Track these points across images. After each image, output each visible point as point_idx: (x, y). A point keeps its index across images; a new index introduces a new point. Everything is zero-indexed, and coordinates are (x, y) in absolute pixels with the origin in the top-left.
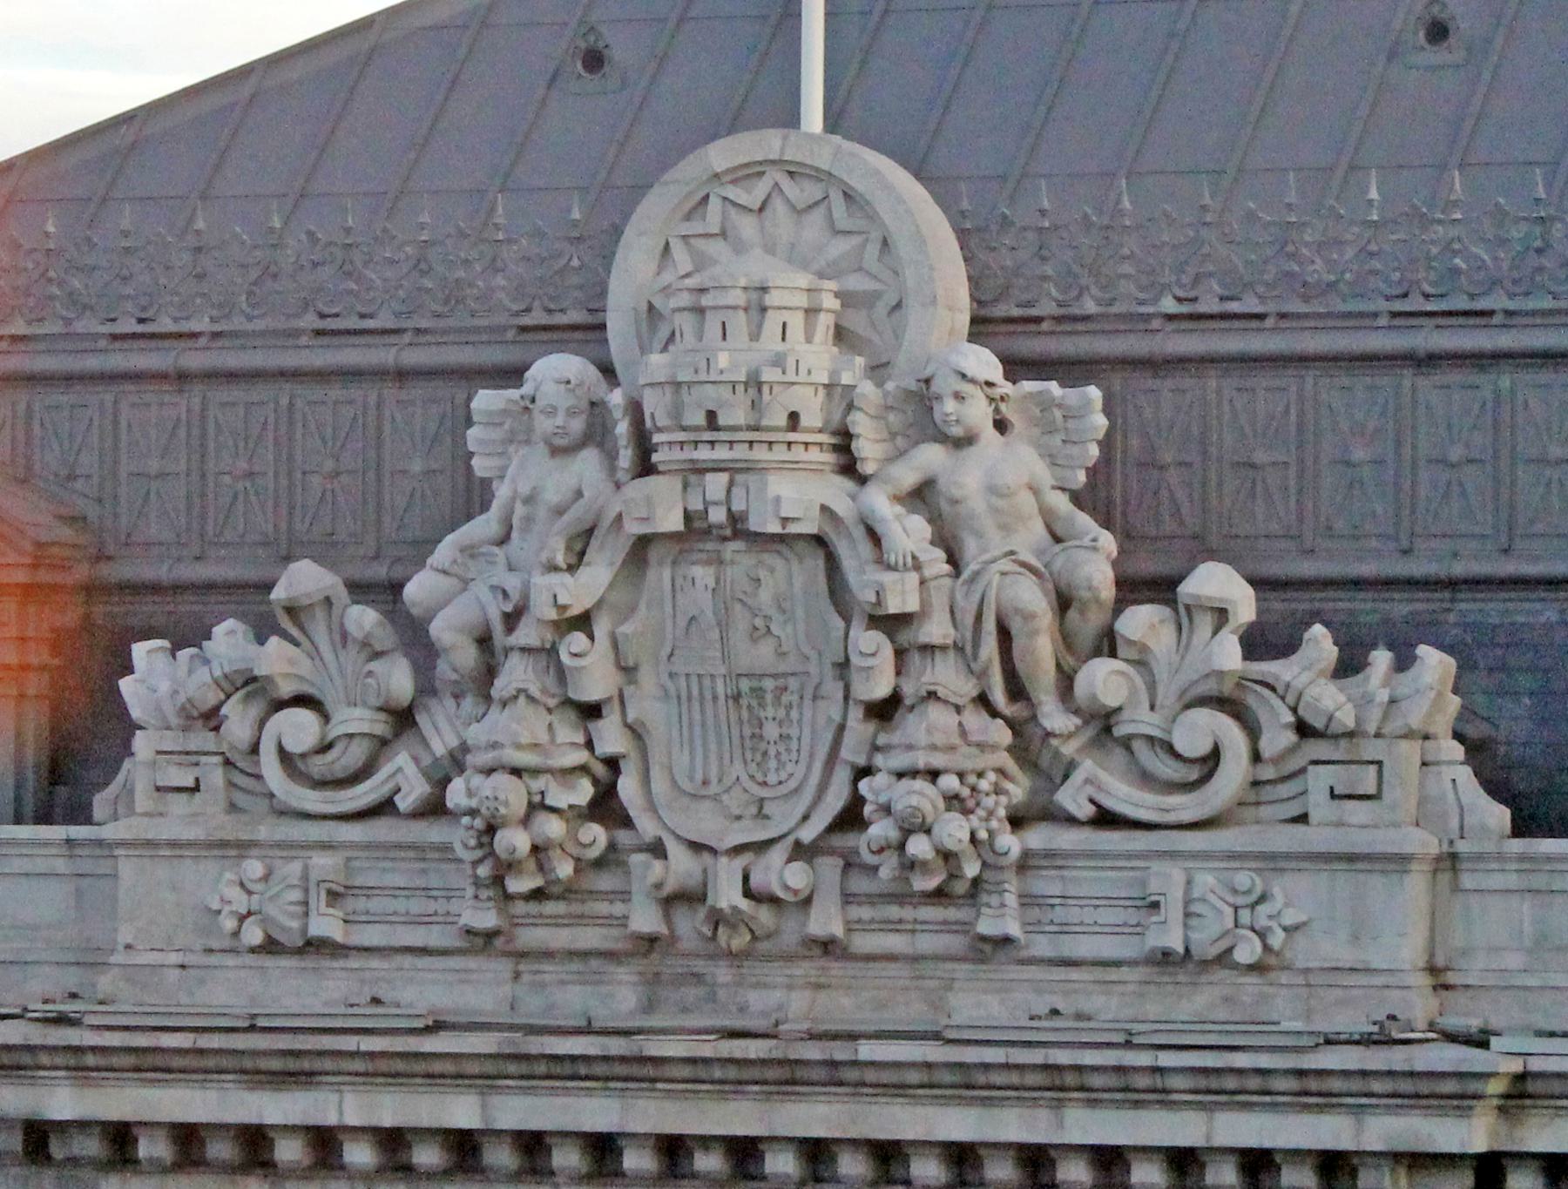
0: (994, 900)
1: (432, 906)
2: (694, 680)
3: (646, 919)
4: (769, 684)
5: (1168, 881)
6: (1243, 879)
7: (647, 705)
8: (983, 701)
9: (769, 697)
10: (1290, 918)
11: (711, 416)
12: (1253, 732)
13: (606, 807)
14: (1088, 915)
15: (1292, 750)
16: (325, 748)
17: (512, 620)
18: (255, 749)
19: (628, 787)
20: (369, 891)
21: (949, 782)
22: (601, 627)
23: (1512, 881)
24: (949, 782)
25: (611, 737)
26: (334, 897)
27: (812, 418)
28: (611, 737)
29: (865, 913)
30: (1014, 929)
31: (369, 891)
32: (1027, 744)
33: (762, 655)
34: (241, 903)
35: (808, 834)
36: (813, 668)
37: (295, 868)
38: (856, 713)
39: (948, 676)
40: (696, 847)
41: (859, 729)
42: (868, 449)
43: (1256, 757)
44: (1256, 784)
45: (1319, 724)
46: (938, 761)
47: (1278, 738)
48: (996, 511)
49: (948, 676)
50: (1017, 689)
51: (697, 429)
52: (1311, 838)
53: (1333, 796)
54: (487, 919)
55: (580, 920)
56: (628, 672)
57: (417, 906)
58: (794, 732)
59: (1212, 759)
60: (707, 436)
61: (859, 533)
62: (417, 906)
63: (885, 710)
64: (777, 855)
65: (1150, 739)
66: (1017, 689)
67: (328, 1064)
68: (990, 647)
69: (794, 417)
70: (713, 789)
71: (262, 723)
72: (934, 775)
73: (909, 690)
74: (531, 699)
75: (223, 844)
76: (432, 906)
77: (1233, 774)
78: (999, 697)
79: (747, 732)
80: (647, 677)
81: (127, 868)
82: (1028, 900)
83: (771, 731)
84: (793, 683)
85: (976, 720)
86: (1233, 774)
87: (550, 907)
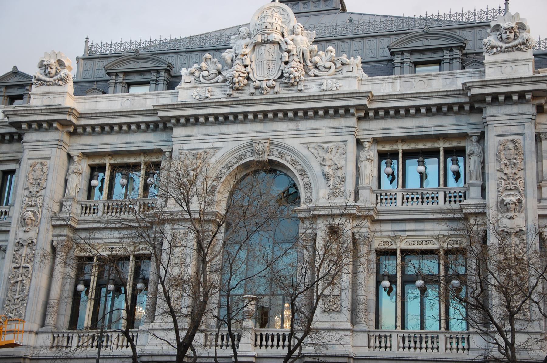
3: (252, 91)
5: (324, 82)
6: (334, 80)
7: (253, 66)
8: (300, 62)
10: (340, 85)
12: (335, 64)
13: (248, 78)
15: (340, 67)
17: (236, 56)
18: (199, 77)
19: (251, 75)
20: (214, 92)
21: (296, 68)
22: (249, 56)
25: (249, 69)
26: (209, 92)
27: (279, 28)
30: (303, 88)
31: (214, 92)
32: (306, 67)
33: (270, 58)
34: (196, 94)
35: (275, 78)
37: (204, 89)
39: (295, 58)
40: (260, 81)
42: (286, 34)
43: (336, 68)
46: (294, 66)
47: (339, 65)
49: (295, 58)
50: (304, 60)
52: (344, 76)
55: (243, 93)
56: (252, 62)
57: (220, 93)
61: (284, 42)
62: (220, 93)
63: (286, 63)
66: (304, 60)
67: (209, 105)
68: (301, 54)
69: (277, 28)
72: (294, 68)
73: (290, 60)
75: (194, 87)
78: (302, 61)
80: (254, 62)
81: (180, 92)
82: (304, 86)
83: (271, 68)
85: (299, 64)
87: (239, 92)
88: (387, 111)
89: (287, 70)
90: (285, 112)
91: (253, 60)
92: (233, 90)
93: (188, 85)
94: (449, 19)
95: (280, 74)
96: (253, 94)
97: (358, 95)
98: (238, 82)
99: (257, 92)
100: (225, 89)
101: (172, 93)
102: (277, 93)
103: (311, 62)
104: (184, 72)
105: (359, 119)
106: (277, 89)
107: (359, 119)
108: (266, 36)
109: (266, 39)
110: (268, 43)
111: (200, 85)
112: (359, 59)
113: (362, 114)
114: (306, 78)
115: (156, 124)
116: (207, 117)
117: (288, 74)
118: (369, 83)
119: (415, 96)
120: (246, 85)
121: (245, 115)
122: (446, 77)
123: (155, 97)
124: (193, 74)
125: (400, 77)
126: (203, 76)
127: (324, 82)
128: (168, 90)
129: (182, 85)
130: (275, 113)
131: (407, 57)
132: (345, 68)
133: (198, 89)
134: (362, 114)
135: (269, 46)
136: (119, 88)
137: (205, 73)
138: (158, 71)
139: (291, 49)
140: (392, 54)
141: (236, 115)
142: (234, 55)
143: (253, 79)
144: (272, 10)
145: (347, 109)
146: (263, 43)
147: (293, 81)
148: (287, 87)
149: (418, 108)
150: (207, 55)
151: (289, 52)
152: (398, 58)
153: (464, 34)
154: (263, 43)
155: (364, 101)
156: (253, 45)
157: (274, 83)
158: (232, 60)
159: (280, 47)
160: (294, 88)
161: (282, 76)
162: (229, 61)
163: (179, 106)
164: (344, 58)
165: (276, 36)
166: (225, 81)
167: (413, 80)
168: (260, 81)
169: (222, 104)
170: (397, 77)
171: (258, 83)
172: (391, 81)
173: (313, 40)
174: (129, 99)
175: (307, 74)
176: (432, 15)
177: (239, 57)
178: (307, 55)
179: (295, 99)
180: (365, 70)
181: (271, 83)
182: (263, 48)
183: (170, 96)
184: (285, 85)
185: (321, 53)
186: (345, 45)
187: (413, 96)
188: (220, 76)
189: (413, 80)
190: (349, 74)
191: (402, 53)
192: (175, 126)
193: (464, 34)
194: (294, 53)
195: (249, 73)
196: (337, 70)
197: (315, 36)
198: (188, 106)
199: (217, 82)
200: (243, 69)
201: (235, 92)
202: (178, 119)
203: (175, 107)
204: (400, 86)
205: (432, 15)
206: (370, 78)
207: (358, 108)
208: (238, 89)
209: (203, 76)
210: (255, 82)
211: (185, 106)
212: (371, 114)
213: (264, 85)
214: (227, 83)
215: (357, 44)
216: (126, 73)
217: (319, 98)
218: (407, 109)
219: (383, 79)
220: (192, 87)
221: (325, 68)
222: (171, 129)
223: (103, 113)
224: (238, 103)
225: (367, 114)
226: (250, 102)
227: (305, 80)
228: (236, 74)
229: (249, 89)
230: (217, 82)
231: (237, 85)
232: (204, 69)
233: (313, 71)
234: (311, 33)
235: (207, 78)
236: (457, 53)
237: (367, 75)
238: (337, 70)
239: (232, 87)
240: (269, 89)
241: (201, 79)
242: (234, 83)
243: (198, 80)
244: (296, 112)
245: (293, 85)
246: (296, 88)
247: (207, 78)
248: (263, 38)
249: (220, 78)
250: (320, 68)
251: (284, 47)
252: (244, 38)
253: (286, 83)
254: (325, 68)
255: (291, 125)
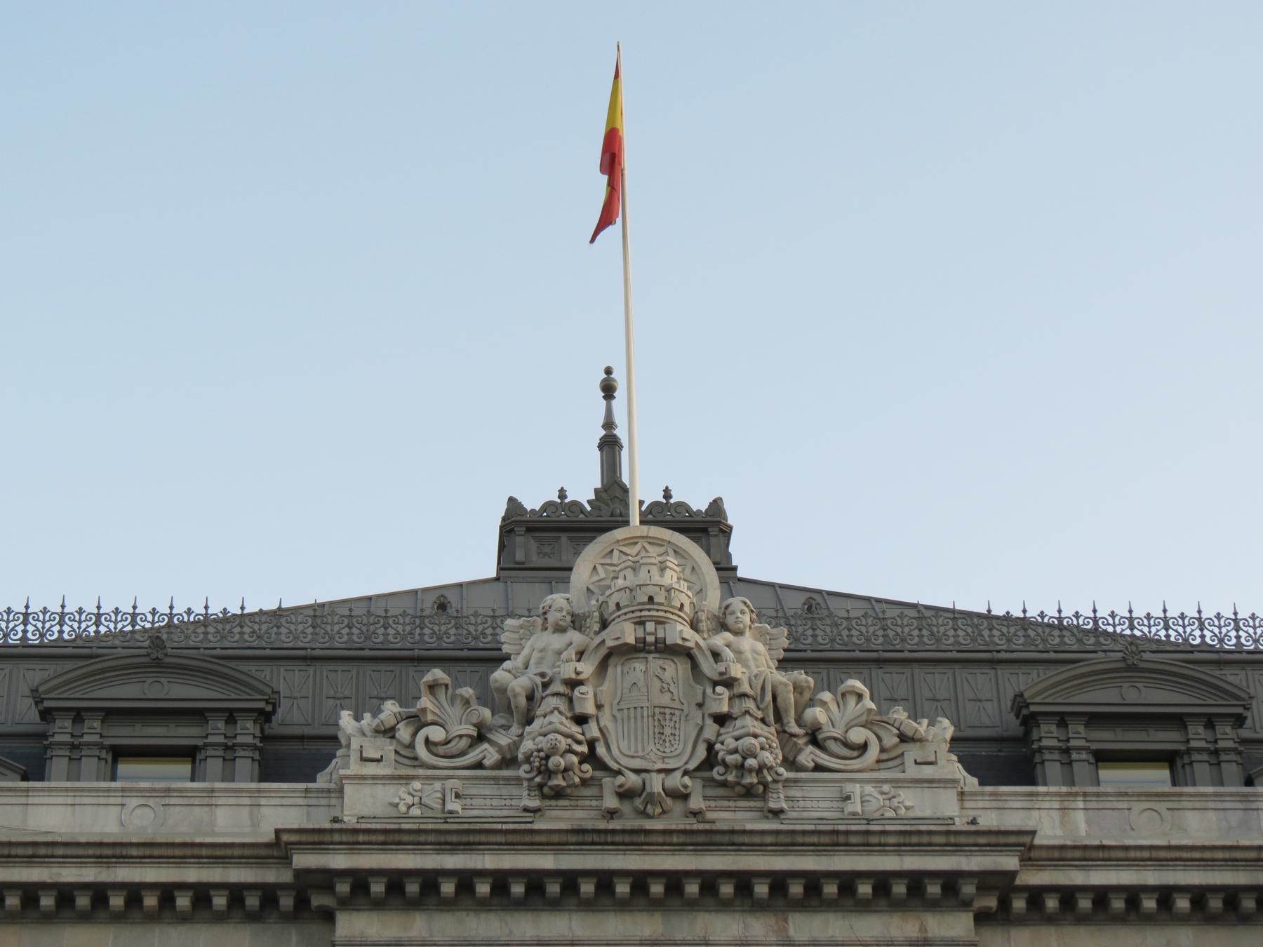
0: (775, 796)
1: (503, 802)
2: (632, 711)
3: (611, 802)
4: (668, 711)
6: (886, 788)
7: (606, 720)
8: (763, 721)
9: (668, 717)
10: (908, 803)
11: (651, 599)
14: (815, 804)
15: (896, 746)
16: (447, 742)
17: (545, 686)
18: (411, 746)
19: (601, 750)
20: (472, 797)
23: (987, 804)
24: (762, 740)
25: (593, 730)
26: (457, 796)
27: (687, 608)
28: (593, 730)
29: (713, 804)
30: (785, 806)
31: (472, 797)
33: (665, 700)
34: (409, 800)
35: (692, 766)
36: (685, 707)
38: (709, 721)
39: (750, 704)
40: (637, 771)
41: (711, 730)
44: (878, 761)
45: (910, 734)
47: (891, 740)
48: (755, 659)
49: (750, 704)
50: (778, 718)
51: (643, 604)
53: (916, 763)
54: (535, 803)
55: (575, 808)
56: (599, 707)
57: (495, 802)
58: (677, 733)
59: (863, 748)
60: (648, 607)
61: (708, 654)
62: (495, 802)
64: (678, 774)
65: (835, 739)
66: (778, 718)
68: (769, 697)
70: (640, 754)
71: (415, 734)
72: (756, 736)
74: (560, 713)
75: (400, 777)
76: (503, 802)
77: (873, 753)
79: (657, 731)
80: (607, 709)
83: (667, 731)
84: (677, 713)
86: (873, 753)
87: (562, 802)
88: (1068, 895)
89: (731, 743)
90: (744, 881)
91: (604, 700)
92: (544, 797)
93: (372, 769)
94: (1128, 632)
95: (701, 753)
96: (612, 814)
97: (993, 840)
98: (566, 770)
99: (626, 808)
100: (514, 790)
101: (307, 790)
102: (695, 814)
103: (799, 722)
104: (346, 719)
105: (982, 918)
106: (696, 803)
107: (982, 918)
108: (650, 626)
109: (650, 639)
110: (657, 651)
111: (421, 772)
112: (946, 729)
113: (991, 902)
114: (792, 775)
115: (269, 894)
116: (465, 880)
117: (737, 757)
118: (987, 804)
119: (1162, 854)
120: (584, 782)
121: (605, 880)
122: (1227, 805)
123: (247, 801)
124: (390, 732)
125: (1085, 794)
126: (427, 741)
127: (856, 790)
128: (263, 779)
129: (347, 766)
130: (709, 881)
131: (1079, 735)
132: (912, 752)
133: (417, 785)
134: (991, 902)
135: (660, 662)
136: (89, 764)
137: (437, 734)
138: (231, 716)
139: (739, 676)
140: (1030, 720)
141: (570, 880)
142: (539, 680)
143: (615, 766)
144: (638, 547)
145: (950, 881)
146: (639, 649)
147: (751, 779)
148: (728, 798)
149: (1165, 895)
150: (437, 674)
151: (729, 683)
152: (1048, 735)
153: (1234, 677)
154: (639, 649)
155: (1010, 862)
156: (603, 652)
157: (687, 780)
158: (530, 697)
159: (695, 666)
160: (752, 804)
161: (711, 760)
162: (522, 701)
163: (373, 838)
164: (900, 714)
165: (679, 632)
166: (508, 761)
167: (1125, 805)
168: (637, 771)
169: (528, 839)
170: (1076, 794)
171: (633, 780)
172: (1057, 805)
173: (781, 654)
174: (151, 802)
175: (791, 763)
176: (1077, 615)
177: (558, 687)
178: (789, 699)
179: (782, 839)
180: (970, 765)
181: (676, 781)
182: (639, 666)
183: (300, 801)
184: (721, 792)
185: (826, 696)
186: (897, 679)
187: (1155, 854)
188: (486, 745)
189: (1125, 805)
190: (928, 771)
191: (1062, 720)
192: (346, 903)
193: (1234, 677)
194: (745, 688)
195: (592, 744)
196: (885, 756)
197: (785, 643)
198: (405, 838)
199: (479, 765)
200: (575, 729)
201: (547, 802)
202: (360, 880)
203: (361, 838)
204: (1088, 822)
205: (1077, 615)
206: (989, 789)
207: (987, 881)
208: (558, 794)
209: (427, 741)
210: (619, 773)
211: (391, 838)
212: (1019, 904)
213: (656, 784)
214: (522, 772)
215: (939, 681)
216: (112, 715)
217: (835, 840)
218: (1133, 895)
219: (1031, 794)
220: (392, 778)
221: (846, 744)
222: (328, 917)
223: (78, 844)
224: (582, 838)
225: (1005, 904)
226: (627, 839)
227: (787, 780)
228: (563, 743)
229: (600, 797)
230: (479, 765)
231: (558, 781)
232: (430, 717)
233: (808, 755)
234: (775, 631)
235: (441, 750)
236: (1227, 735)
237: (975, 780)
238: (885, 756)
239: (541, 786)
240: (669, 801)
241: (422, 751)
242: (549, 773)
243: (407, 755)
244: (779, 881)
245: (749, 793)
246: (759, 804)
247: (441, 750)
248: (641, 634)
249: (490, 754)
250: (832, 745)
251: (708, 667)
252: (560, 630)
253: (724, 784)
254: (846, 744)
255: (759, 927)
